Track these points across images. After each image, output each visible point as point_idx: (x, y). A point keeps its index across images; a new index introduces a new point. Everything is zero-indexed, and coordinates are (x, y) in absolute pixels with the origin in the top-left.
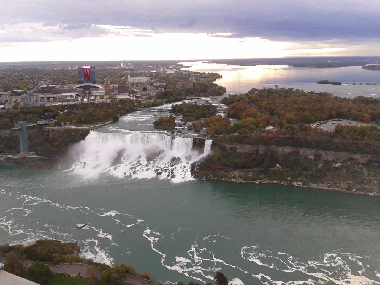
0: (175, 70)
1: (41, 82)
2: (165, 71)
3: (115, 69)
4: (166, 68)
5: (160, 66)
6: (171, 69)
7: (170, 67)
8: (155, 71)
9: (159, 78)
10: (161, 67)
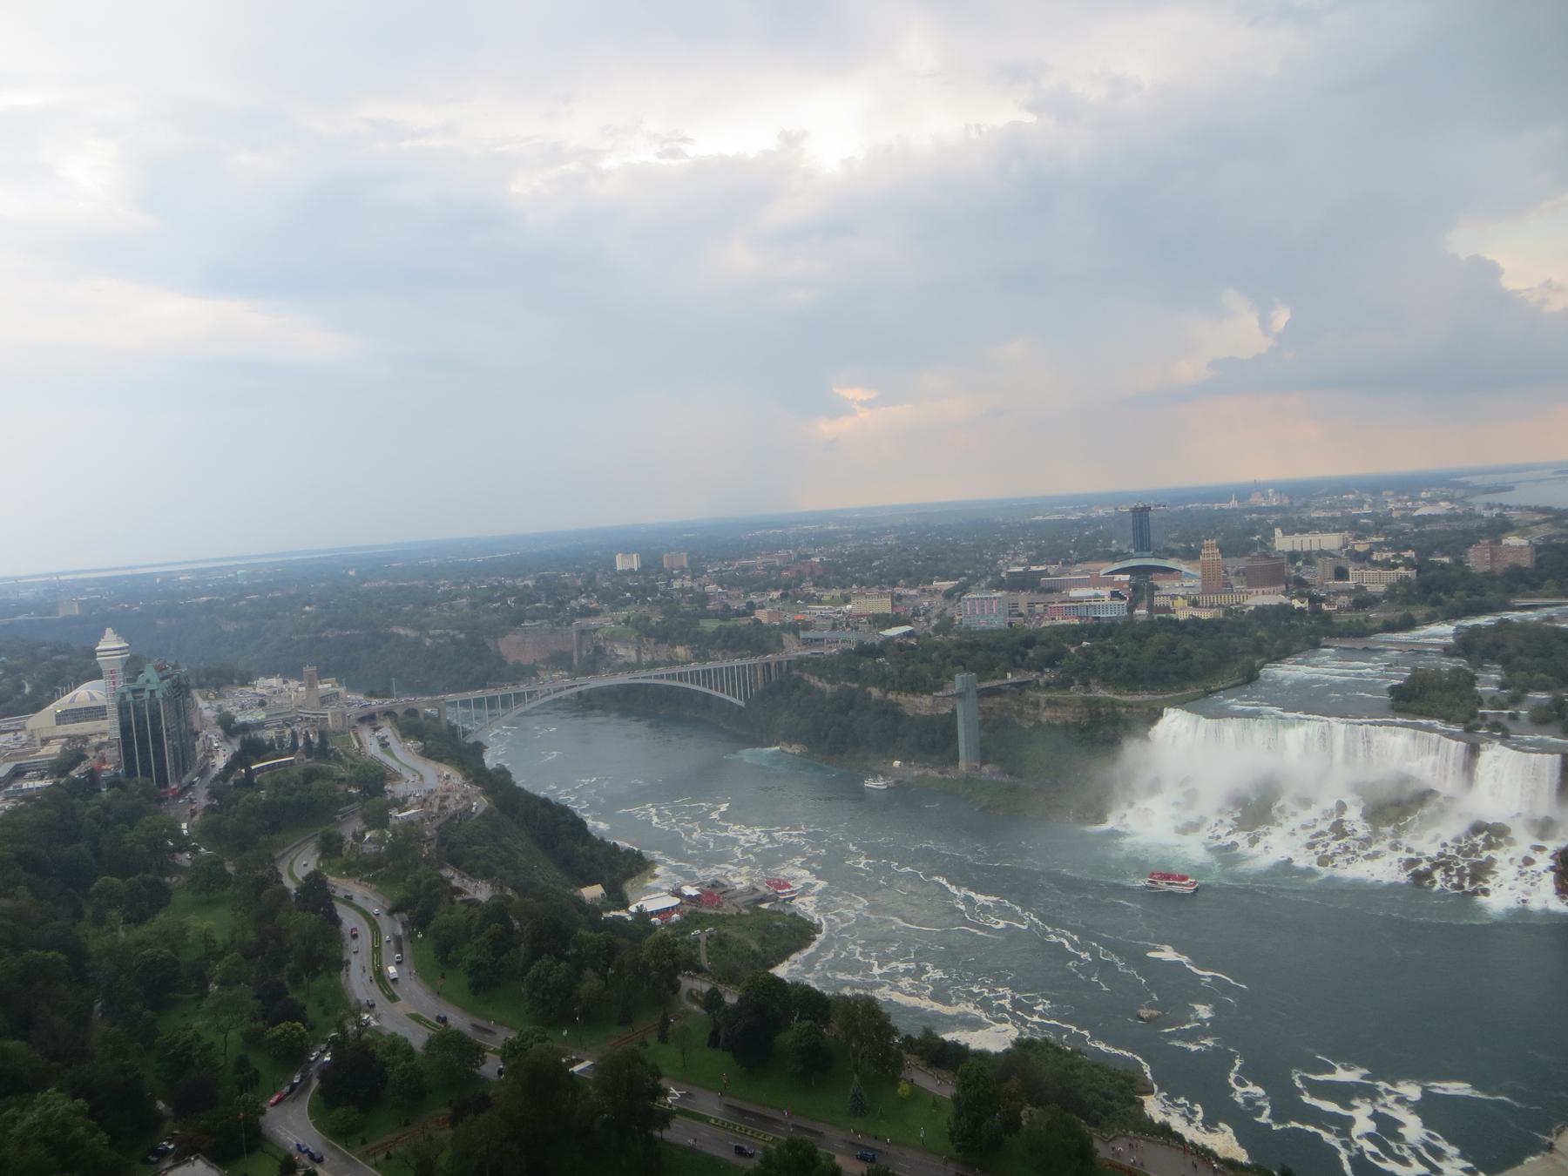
0: (1443, 504)
1: (1003, 559)
2: (1407, 508)
3: (1221, 509)
4: (1406, 497)
5: (1384, 493)
6: (1432, 501)
7: (1423, 495)
8: (1367, 510)
9: (1386, 535)
10: (1389, 496)
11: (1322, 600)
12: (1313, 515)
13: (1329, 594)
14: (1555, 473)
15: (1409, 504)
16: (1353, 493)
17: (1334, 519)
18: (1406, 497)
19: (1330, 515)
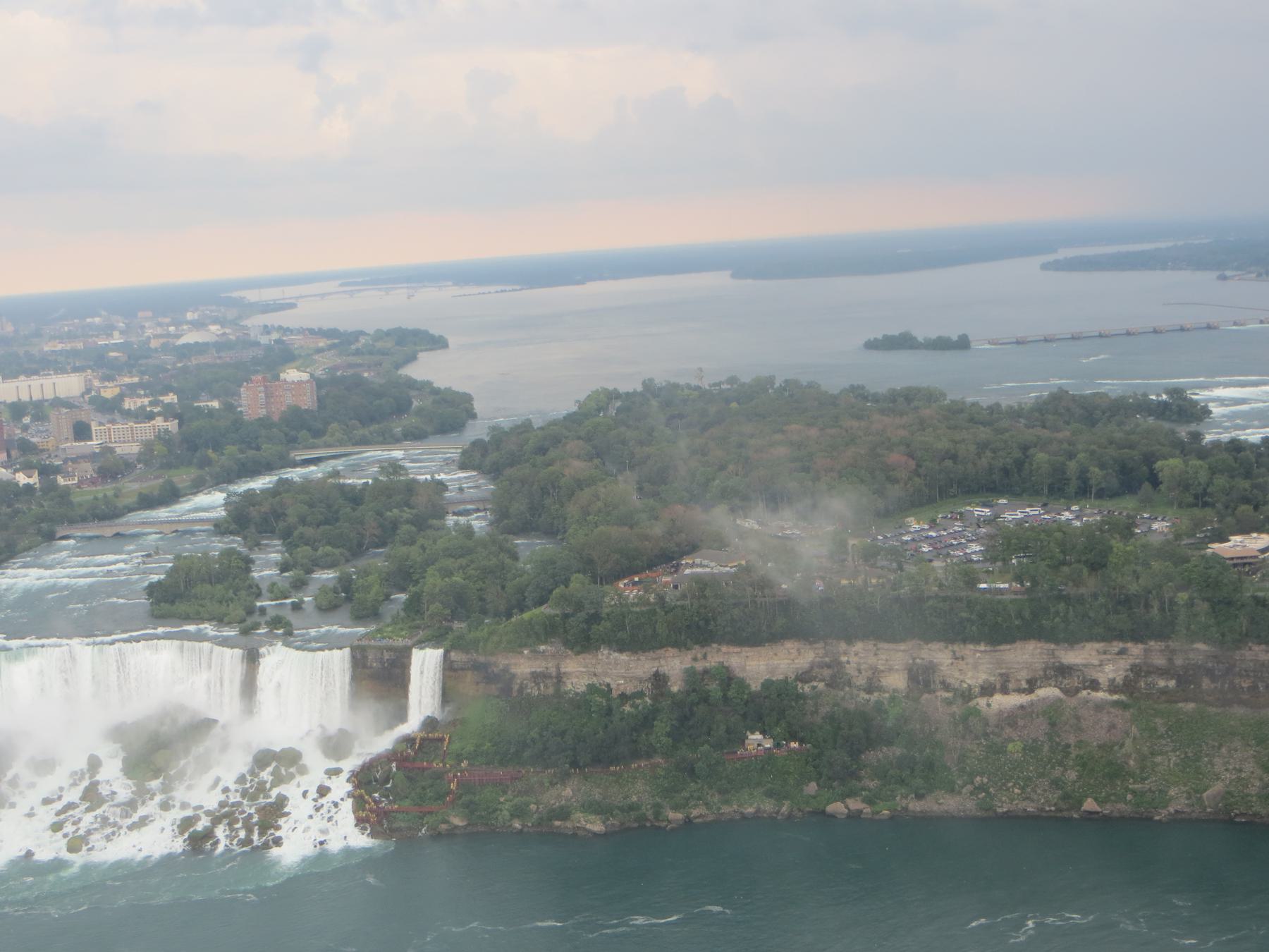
0: (213, 328)
2: (169, 335)
4: (167, 320)
5: (140, 314)
6: (198, 325)
7: (190, 316)
8: (117, 339)
9: (143, 373)
11: (57, 470)
12: (46, 349)
13: (66, 461)
14: (341, 285)
15: (172, 329)
16: (100, 316)
17: (75, 353)
18: (167, 320)
19: (68, 347)
